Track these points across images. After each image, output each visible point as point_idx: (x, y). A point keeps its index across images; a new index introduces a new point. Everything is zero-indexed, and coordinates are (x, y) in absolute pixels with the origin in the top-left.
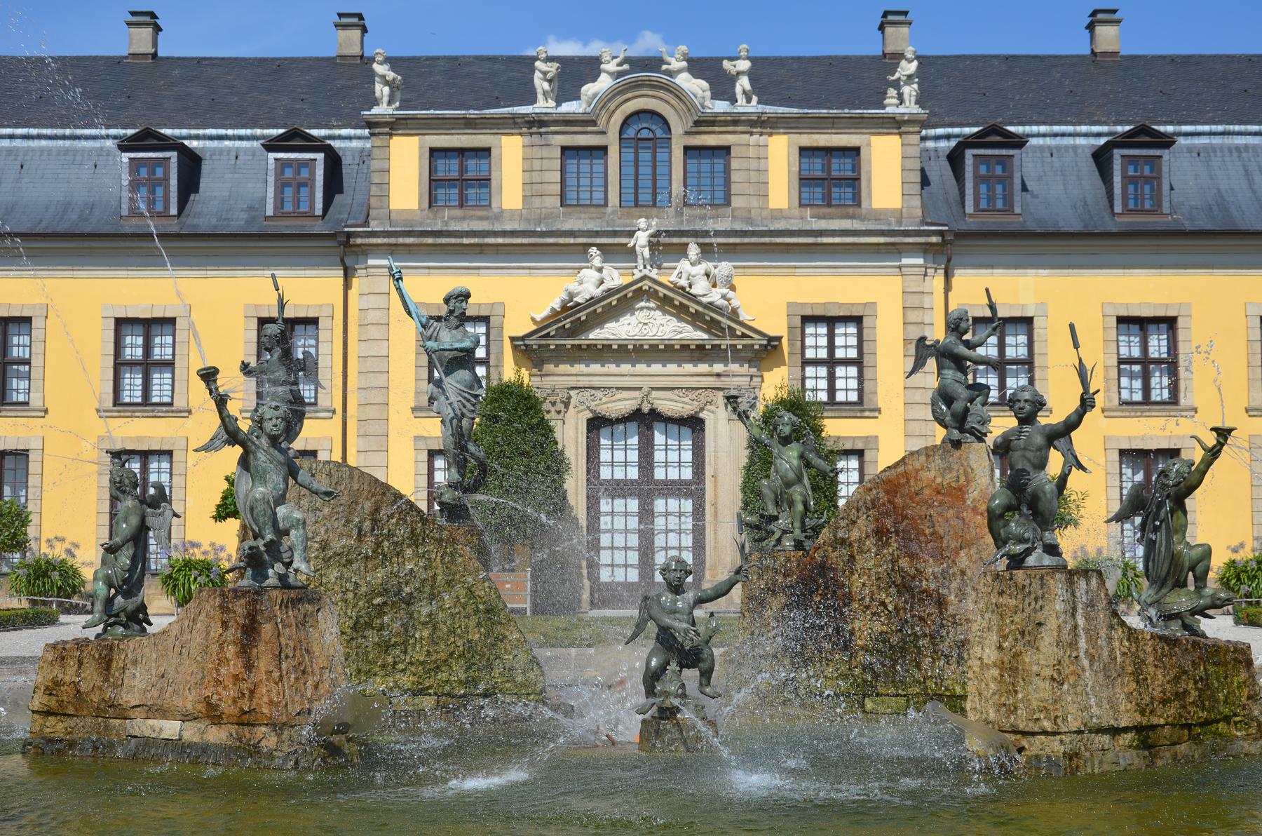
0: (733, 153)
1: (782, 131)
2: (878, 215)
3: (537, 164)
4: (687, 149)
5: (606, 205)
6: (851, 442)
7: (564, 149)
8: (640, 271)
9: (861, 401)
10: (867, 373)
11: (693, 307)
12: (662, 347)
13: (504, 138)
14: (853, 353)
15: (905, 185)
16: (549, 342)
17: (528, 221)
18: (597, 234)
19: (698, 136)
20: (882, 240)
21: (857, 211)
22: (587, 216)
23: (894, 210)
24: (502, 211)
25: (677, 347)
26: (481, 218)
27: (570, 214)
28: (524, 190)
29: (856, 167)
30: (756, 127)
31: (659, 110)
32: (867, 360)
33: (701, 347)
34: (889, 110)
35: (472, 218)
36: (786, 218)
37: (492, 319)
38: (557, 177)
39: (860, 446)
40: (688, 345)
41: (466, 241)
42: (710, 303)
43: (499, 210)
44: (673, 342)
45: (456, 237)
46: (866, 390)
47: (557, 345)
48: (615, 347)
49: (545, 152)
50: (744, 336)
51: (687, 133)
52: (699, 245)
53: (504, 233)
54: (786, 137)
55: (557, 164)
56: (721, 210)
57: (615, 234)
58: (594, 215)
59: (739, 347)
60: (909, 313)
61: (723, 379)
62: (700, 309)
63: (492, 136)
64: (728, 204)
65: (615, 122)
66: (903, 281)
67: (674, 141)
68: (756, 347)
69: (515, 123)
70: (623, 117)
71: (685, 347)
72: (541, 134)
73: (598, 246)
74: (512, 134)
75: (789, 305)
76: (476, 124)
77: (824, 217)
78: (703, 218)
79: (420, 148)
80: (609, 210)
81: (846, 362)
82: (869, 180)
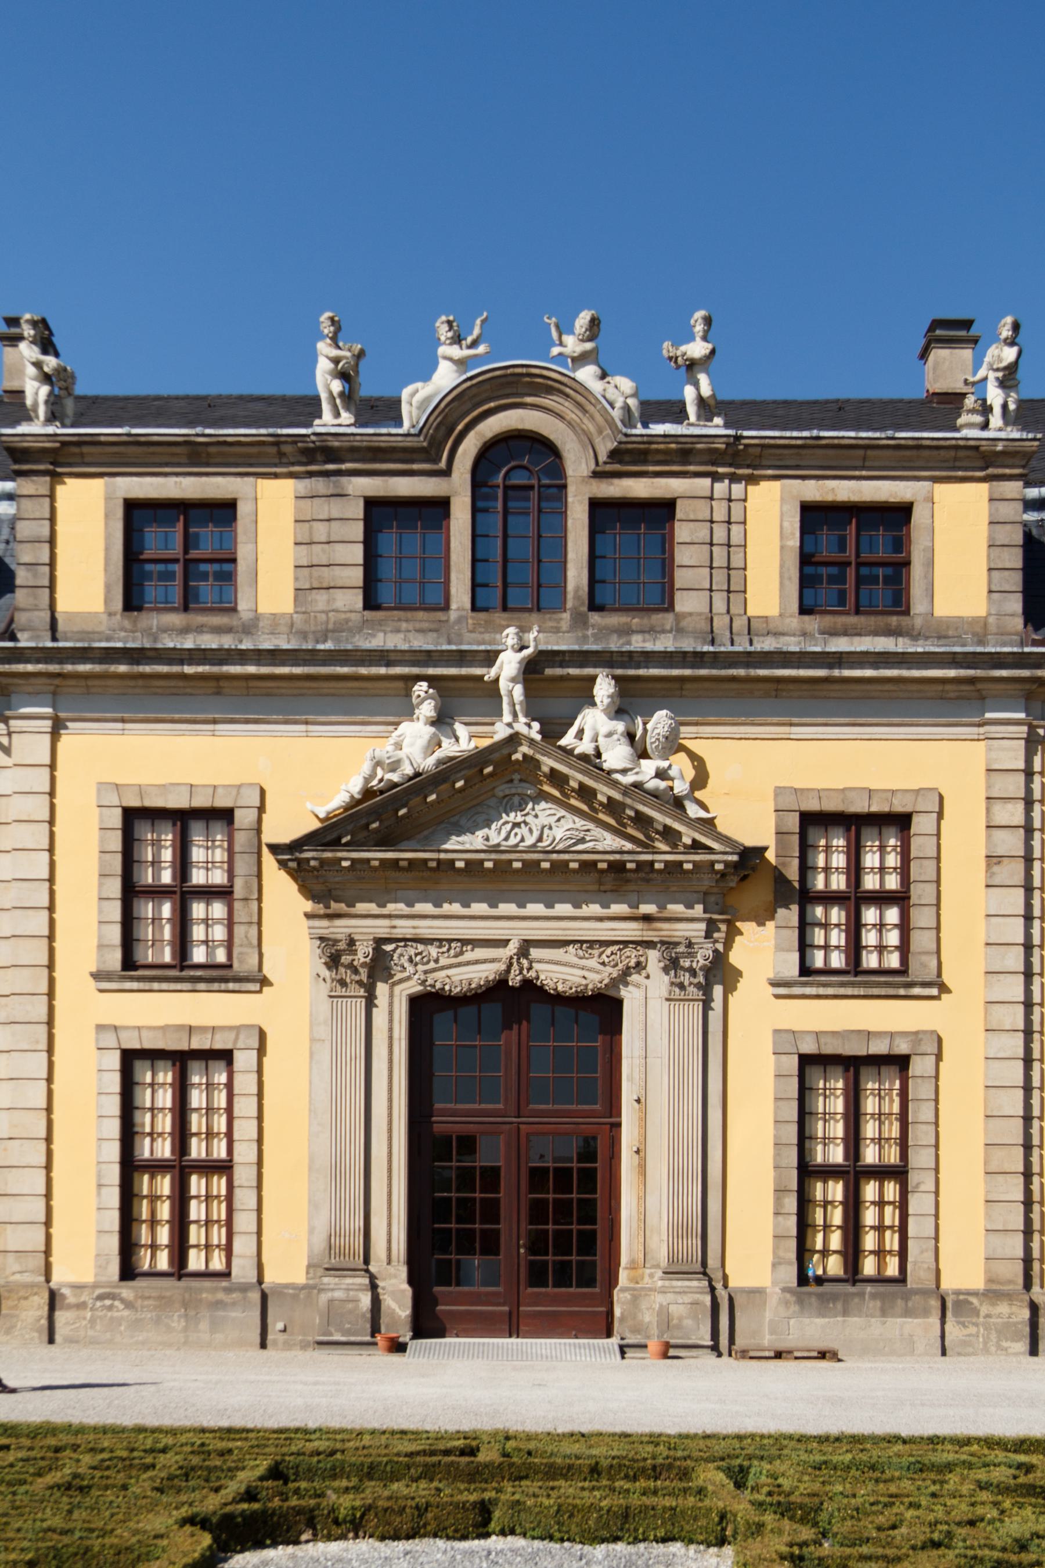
0: (679, 514)
1: (770, 472)
2: (942, 630)
3: (321, 531)
4: (596, 505)
5: (446, 607)
6: (887, 1041)
7: (372, 504)
8: (509, 725)
9: (903, 971)
10: (921, 918)
11: (604, 792)
12: (545, 865)
13: (264, 484)
14: (892, 882)
15: (995, 573)
16: (340, 855)
17: (304, 635)
18: (428, 657)
19: (616, 481)
20: (952, 673)
21: (904, 620)
22: (410, 626)
23: (975, 620)
24: (257, 618)
25: (574, 865)
26: (218, 630)
27: (380, 622)
28: (296, 579)
29: (901, 543)
30: (723, 465)
31: (545, 432)
32: (920, 893)
33: (616, 867)
34: (966, 433)
35: (200, 629)
36: (777, 634)
37: (238, 814)
38: (357, 553)
39: (902, 1047)
40: (595, 863)
41: (188, 669)
42: (638, 786)
43: (251, 615)
44: (566, 857)
45: (170, 662)
46: (913, 947)
47: (354, 861)
48: (460, 864)
49: (335, 508)
50: (696, 846)
51: (597, 475)
52: (617, 679)
53: (259, 656)
54: (776, 485)
55: (357, 531)
56: (657, 618)
57: (462, 658)
58: (425, 625)
59: (688, 866)
60: (997, 807)
61: (659, 925)
62: (617, 796)
63: (238, 480)
64: (670, 607)
65: (465, 452)
66: (989, 749)
67: (571, 490)
68: (719, 867)
69: (281, 454)
70: (479, 444)
71: (588, 866)
72: (327, 474)
73: (431, 680)
74: (276, 476)
75: (779, 791)
76: (208, 455)
77: (845, 633)
78: (626, 632)
79: (108, 499)
80: (453, 615)
81: (882, 899)
82: (930, 563)
